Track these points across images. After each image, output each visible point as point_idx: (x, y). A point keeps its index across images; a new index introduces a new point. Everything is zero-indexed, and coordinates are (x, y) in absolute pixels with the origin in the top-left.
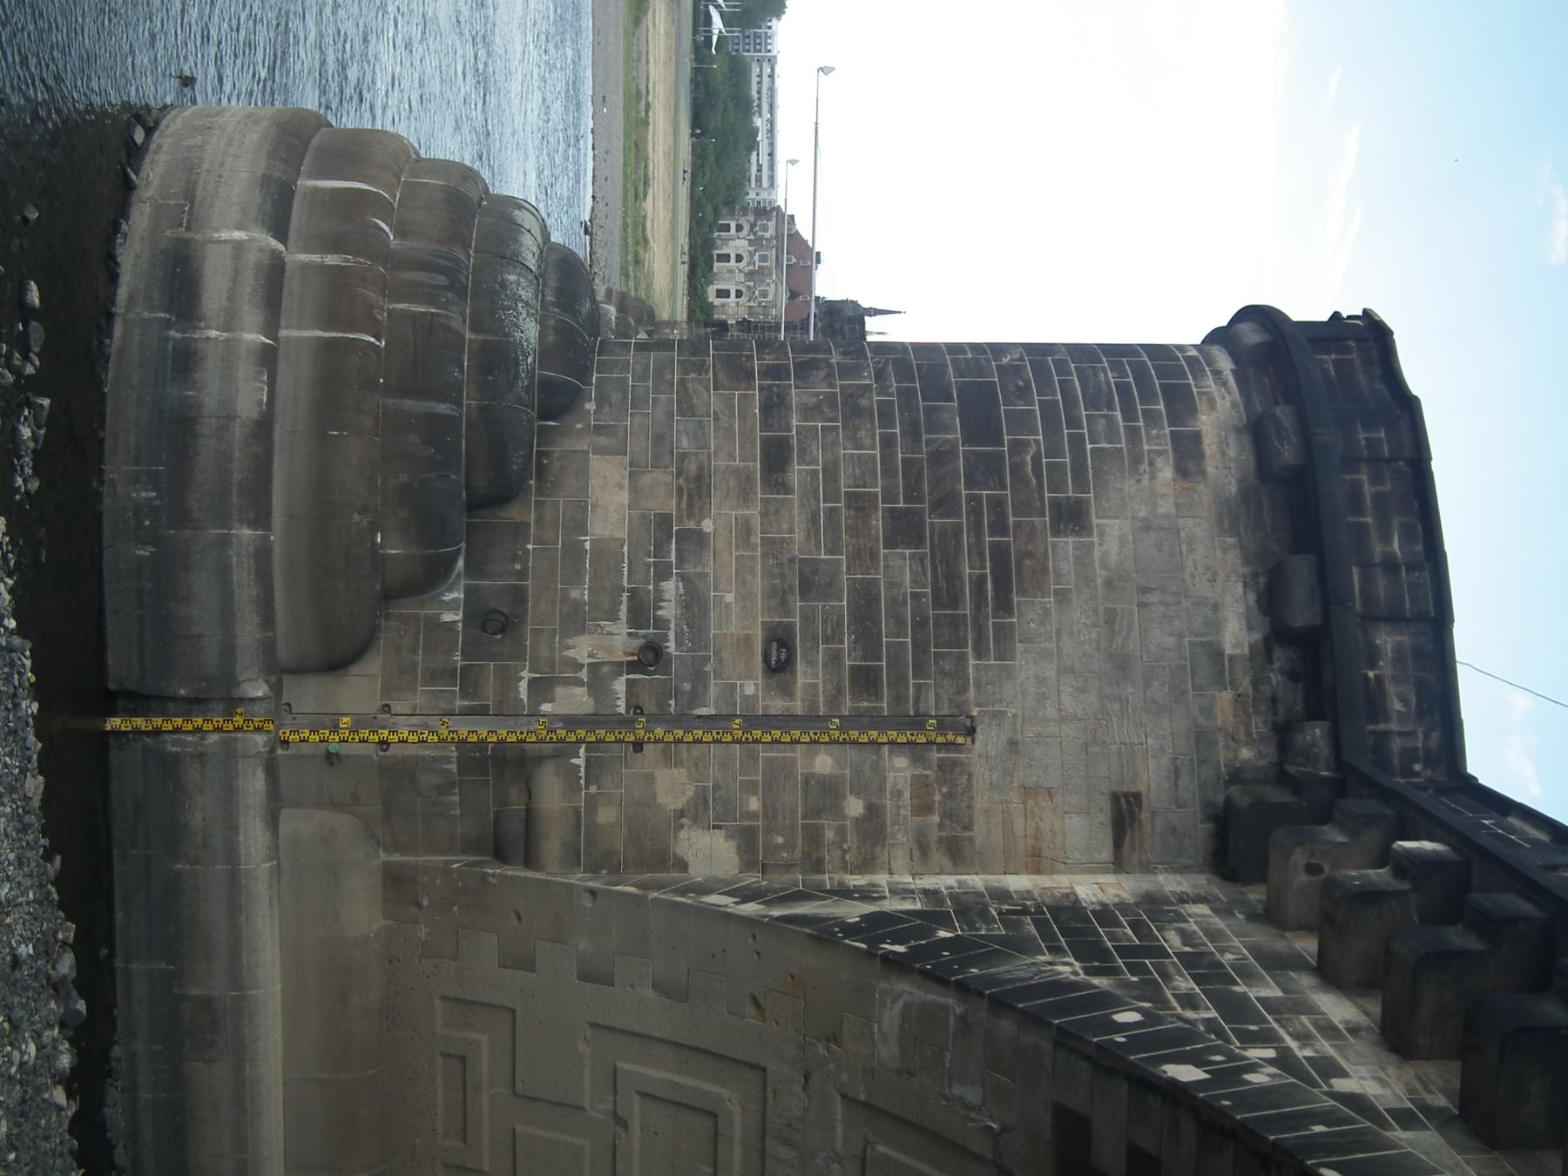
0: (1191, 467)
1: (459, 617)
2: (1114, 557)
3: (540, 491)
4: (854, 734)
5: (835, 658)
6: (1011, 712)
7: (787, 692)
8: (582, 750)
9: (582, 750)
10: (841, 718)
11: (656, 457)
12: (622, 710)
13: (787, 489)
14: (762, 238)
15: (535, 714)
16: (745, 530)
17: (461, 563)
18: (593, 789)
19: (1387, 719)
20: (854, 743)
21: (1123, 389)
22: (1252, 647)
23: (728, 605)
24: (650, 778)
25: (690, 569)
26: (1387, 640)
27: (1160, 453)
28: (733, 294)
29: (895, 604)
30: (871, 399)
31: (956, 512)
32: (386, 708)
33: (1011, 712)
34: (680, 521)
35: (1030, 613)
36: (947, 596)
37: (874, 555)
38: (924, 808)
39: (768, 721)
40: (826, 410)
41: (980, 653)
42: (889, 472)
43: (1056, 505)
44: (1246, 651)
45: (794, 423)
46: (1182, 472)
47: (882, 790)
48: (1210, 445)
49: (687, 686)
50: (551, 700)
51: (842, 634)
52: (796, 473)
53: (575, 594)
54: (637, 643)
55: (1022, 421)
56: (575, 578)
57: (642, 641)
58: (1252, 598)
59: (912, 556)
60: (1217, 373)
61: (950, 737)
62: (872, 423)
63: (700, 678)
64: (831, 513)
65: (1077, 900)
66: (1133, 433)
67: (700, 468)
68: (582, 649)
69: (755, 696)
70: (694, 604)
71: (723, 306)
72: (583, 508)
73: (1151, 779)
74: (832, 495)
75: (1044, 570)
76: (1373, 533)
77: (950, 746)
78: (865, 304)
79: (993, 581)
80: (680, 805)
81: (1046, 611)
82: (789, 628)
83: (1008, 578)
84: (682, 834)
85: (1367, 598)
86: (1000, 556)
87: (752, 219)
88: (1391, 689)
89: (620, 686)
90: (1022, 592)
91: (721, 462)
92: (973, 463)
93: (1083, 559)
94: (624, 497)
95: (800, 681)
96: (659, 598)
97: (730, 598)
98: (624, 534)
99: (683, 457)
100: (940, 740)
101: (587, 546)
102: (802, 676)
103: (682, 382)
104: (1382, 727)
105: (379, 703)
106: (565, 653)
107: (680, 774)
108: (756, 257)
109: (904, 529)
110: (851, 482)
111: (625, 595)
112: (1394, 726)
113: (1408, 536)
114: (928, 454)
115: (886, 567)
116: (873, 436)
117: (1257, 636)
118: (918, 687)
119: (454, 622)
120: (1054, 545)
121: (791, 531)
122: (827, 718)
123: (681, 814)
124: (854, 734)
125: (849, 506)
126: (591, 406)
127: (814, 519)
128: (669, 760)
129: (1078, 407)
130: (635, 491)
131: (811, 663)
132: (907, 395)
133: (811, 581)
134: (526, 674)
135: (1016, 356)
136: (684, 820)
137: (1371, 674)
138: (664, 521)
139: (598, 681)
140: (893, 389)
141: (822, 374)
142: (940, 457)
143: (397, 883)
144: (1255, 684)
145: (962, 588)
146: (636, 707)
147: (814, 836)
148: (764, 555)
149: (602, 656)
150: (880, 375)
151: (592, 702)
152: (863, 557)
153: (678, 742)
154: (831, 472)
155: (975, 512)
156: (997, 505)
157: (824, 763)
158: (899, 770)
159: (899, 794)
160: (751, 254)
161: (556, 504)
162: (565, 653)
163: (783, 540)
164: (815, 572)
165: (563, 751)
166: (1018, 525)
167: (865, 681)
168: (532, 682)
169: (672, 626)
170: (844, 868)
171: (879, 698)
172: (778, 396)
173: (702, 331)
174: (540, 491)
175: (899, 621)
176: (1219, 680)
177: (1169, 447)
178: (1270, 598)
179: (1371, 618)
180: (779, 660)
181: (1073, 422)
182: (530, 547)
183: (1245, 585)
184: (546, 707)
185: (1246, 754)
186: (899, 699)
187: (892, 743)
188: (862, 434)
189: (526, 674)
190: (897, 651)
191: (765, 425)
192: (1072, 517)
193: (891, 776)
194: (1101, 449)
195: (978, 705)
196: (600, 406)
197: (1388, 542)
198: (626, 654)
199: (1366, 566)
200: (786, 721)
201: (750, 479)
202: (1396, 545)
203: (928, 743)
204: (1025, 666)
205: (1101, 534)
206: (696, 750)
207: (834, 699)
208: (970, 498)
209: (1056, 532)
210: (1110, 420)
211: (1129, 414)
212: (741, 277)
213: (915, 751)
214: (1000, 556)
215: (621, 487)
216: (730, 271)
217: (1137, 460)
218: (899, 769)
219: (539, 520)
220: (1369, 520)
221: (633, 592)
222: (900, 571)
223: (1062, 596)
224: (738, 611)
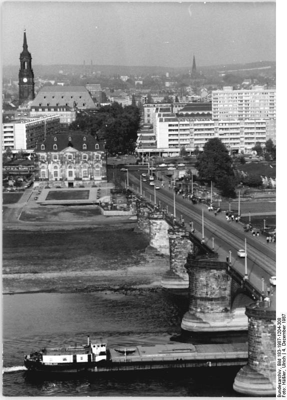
28: (70, 170)
71: (76, 174)
78: (22, 50)
87: (39, 163)
108: (55, 160)
160: (54, 162)
212: (64, 167)
216: (62, 171)
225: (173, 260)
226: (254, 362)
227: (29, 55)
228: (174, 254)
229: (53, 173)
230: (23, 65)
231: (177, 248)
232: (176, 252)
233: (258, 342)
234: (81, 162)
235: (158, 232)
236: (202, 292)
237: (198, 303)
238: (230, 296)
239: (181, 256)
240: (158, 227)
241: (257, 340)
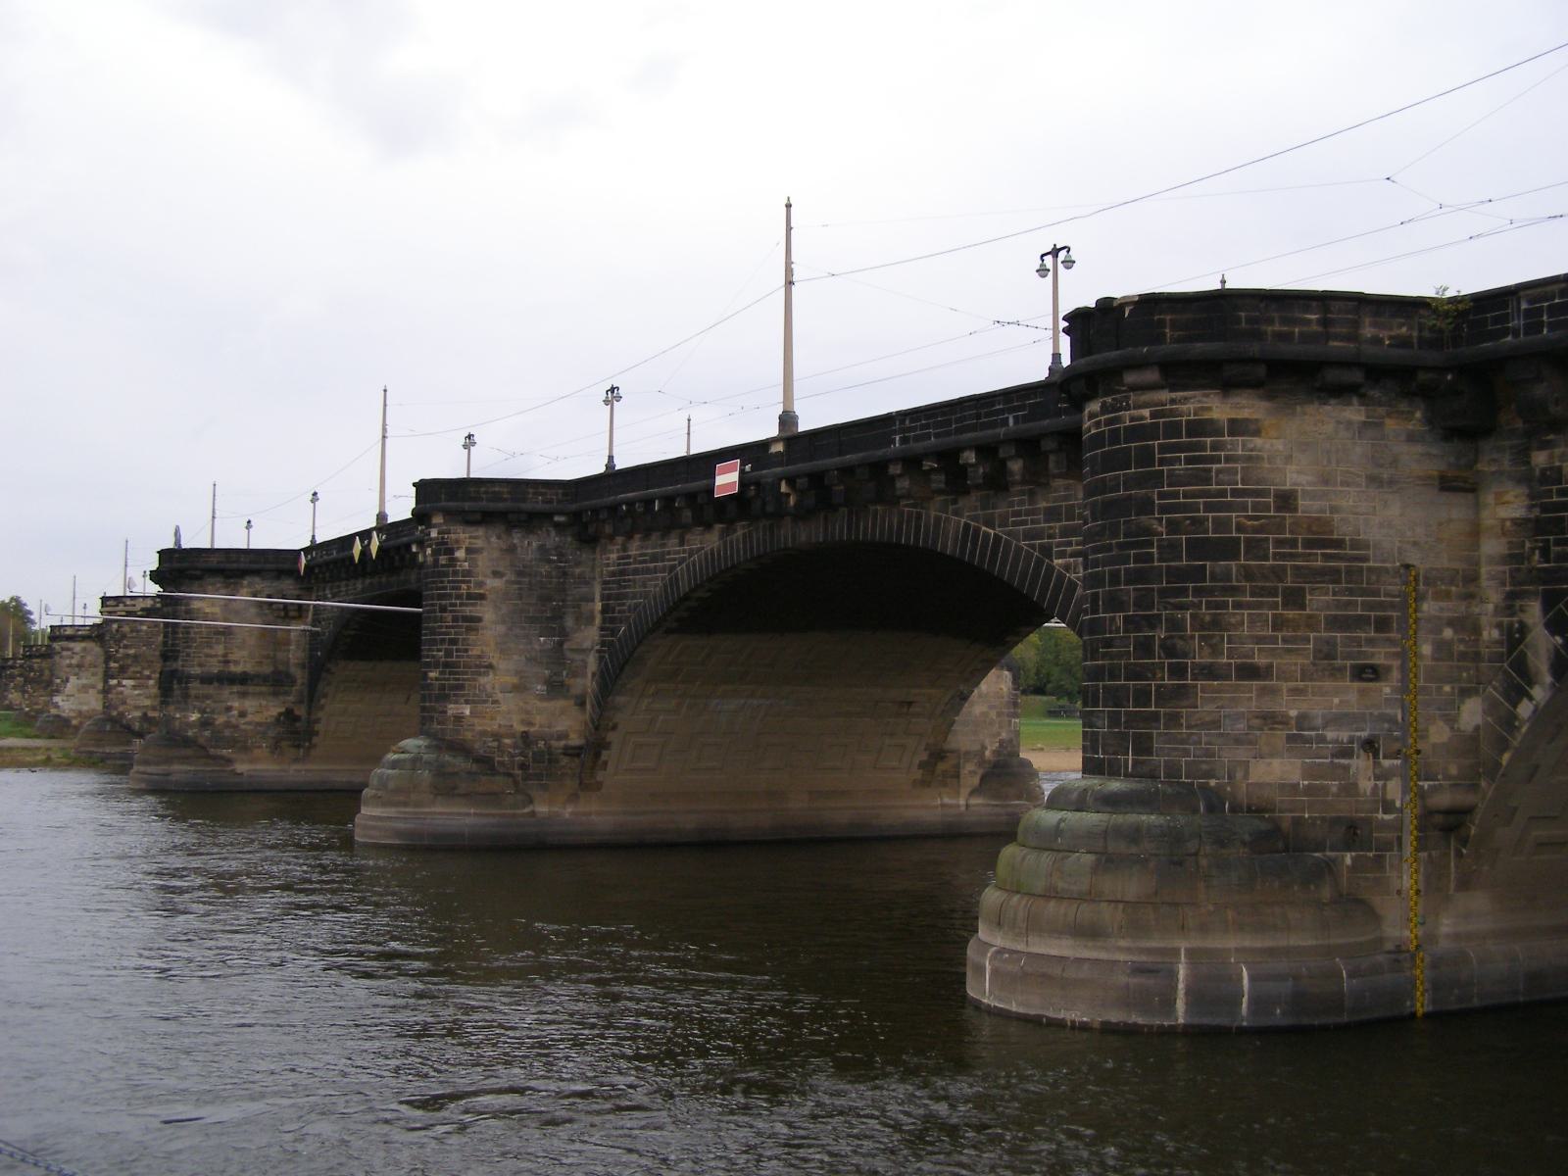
0: (1253, 427)
1: (1348, 855)
2: (1309, 478)
3: (1273, 811)
4: (1411, 632)
5: (1371, 642)
6: (1397, 544)
7: (1388, 669)
8: (1420, 783)
9: (1420, 783)
10: (1402, 639)
11: (1250, 743)
12: (1399, 761)
13: (1271, 666)
15: (1401, 810)
16: (1296, 691)
17: (1317, 854)
18: (1440, 777)
19: (1410, 336)
20: (1415, 633)
21: (1189, 461)
22: (1361, 404)
23: (1341, 701)
24: (1434, 745)
25: (1319, 722)
26: (1368, 331)
27: (1244, 445)
29: (1339, 605)
30: (1204, 614)
31: (1284, 568)
33: (1397, 544)
34: (1290, 729)
35: (1343, 530)
36: (1333, 576)
37: (1310, 617)
38: (1447, 595)
39: (1404, 679)
40: (1214, 641)
41: (1365, 559)
42: (1259, 606)
43: (1278, 509)
44: (1363, 408)
45: (1225, 660)
46: (1257, 433)
47: (1439, 618)
49: (1386, 726)
50: (1393, 802)
51: (1356, 637)
52: (1260, 660)
53: (1334, 789)
55: (1221, 525)
56: (1325, 790)
57: (1362, 751)
59: (1311, 594)
60: (1173, 401)
61: (1412, 578)
62: (1225, 614)
63: (1383, 718)
64: (1285, 641)
65: (1527, 520)
66: (1228, 459)
67: (1257, 717)
68: (1366, 785)
69: (1391, 687)
72: (1282, 787)
73: (1434, 468)
74: (1274, 640)
75: (1318, 519)
76: (1305, 329)
77: (1416, 579)
79: (1326, 548)
80: (1447, 729)
81: (1342, 519)
82: (1352, 666)
83: (1322, 538)
84: (1462, 728)
85: (1349, 338)
86: (1309, 544)
89: (1386, 763)
90: (1332, 532)
91: (1254, 706)
92: (1248, 556)
93: (1313, 496)
94: (1276, 763)
96: (1336, 741)
97: (1336, 701)
98: (1298, 762)
99: (1250, 727)
100: (1413, 584)
101: (1306, 783)
102: (1379, 657)
103: (1188, 728)
104: (1415, 341)
105: (1396, 896)
106: (1368, 793)
107: (1432, 729)
109: (1295, 599)
110: (1266, 628)
111: (1336, 761)
112: (1415, 334)
113: (1308, 310)
114: (1247, 581)
115: (1317, 610)
116: (1235, 614)
117: (1355, 400)
119: (1352, 858)
120: (1303, 512)
121: (1296, 664)
122: (1403, 648)
123: (1452, 728)
124: (1411, 632)
125: (1281, 630)
126: (1213, 782)
127: (1289, 651)
128: (1424, 737)
129: (1209, 489)
130: (1272, 755)
131: (1373, 655)
132: (1198, 592)
133: (1326, 653)
134: (1380, 815)
135: (1155, 522)
136: (1456, 726)
137: (1387, 342)
138: (1291, 738)
139: (1383, 776)
140: (1195, 600)
141: (1180, 644)
142: (1248, 574)
143: (1464, 884)
144: (1380, 406)
145: (1330, 567)
146: (1396, 754)
147: (1463, 656)
148: (1311, 680)
149: (1370, 773)
151: (1395, 779)
152: (1311, 623)
153: (1416, 730)
154: (1259, 640)
155: (1283, 557)
156: (1279, 543)
157: (1426, 649)
158: (1429, 607)
159: (1442, 609)
161: (1282, 802)
162: (1368, 793)
163: (1301, 670)
164: (1320, 651)
165: (1422, 795)
166: (1291, 532)
167: (1383, 625)
168: (1385, 813)
169: (1352, 734)
170: (1477, 640)
171: (1392, 617)
172: (1203, 669)
173: (177, 692)
174: (1273, 811)
175: (1349, 604)
176: (1380, 425)
177: (1240, 439)
179: (1353, 337)
180: (1367, 673)
181: (1222, 493)
182: (1307, 816)
183: (1325, 404)
184: (1398, 804)
185: (1418, 415)
186: (1392, 606)
187: (1416, 611)
188: (1233, 620)
189: (1380, 815)
190: (1367, 606)
191: (1228, 677)
192: (1286, 500)
193: (1433, 612)
194: (1242, 479)
195: (1395, 562)
196: (1213, 777)
198: (1369, 759)
199: (1328, 337)
200: (1403, 669)
202: (1314, 317)
203: (1415, 590)
204: (1372, 534)
205: (1298, 485)
206: (1420, 719)
207: (1392, 642)
208: (1275, 559)
209: (1295, 510)
210: (1219, 472)
211: (1217, 460)
213: (1420, 598)
214: (1309, 544)
215: (1270, 764)
217: (1249, 459)
218: (1429, 607)
219: (1291, 811)
220: (1297, 330)
221: (1334, 756)
222: (1320, 601)
223: (1334, 509)
224: (1345, 696)
225: (114, 682)
226: (452, 709)
228: (116, 665)
231: (126, 647)
232: (122, 658)
233: (466, 619)
235: (76, 674)
236: (207, 656)
237: (193, 692)
238: (303, 666)
239: (139, 669)
240: (74, 662)
241: (468, 611)
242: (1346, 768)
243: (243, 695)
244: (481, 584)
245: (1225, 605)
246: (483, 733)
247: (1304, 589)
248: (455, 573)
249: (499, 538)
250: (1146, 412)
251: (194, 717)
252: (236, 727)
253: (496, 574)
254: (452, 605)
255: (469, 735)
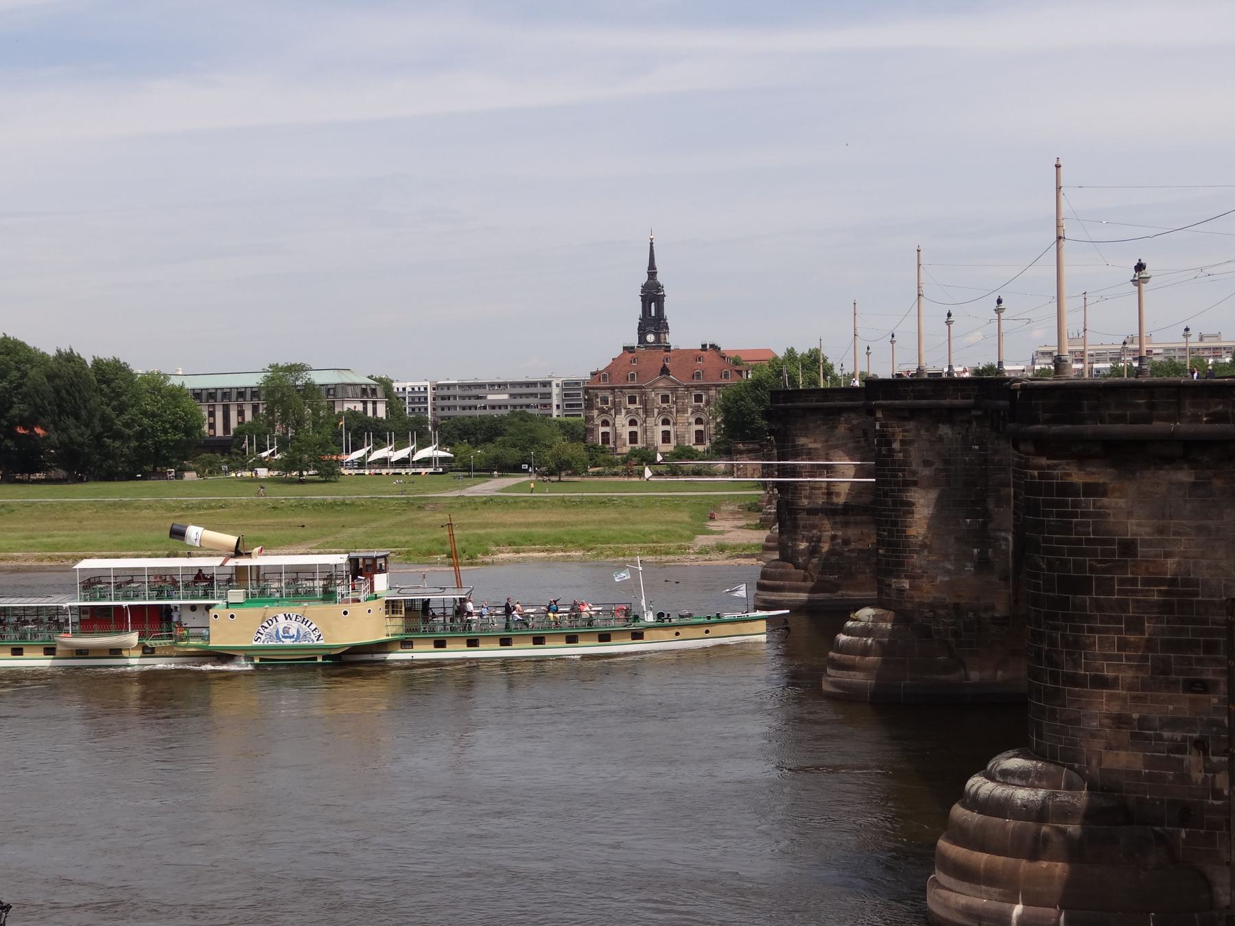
2: (1148, 530)
5: (1200, 661)
7: (1216, 683)
13: (1117, 678)
14: (614, 403)
15: (1229, 797)
17: (1157, 828)
21: (1059, 515)
25: (1157, 723)
28: (667, 428)
31: (1126, 602)
32: (1228, 864)
33: (1224, 582)
41: (1196, 594)
42: (1107, 631)
46: (1104, 494)
48: (1089, 480)
53: (1171, 778)
54: (1194, 751)
58: (1167, 467)
60: (1049, 467)
66: (1084, 515)
68: (1198, 776)
70: (1174, 724)
71: (677, 437)
74: (1119, 658)
78: (644, 278)
87: (596, 413)
88: (1211, 411)
89: (1215, 759)
90: (1166, 573)
93: (1149, 544)
94: (1123, 754)
95: (1211, 677)
96: (1171, 740)
97: (1171, 707)
99: (1101, 725)
103: (1061, 722)
108: (632, 407)
118: (1214, 623)
130: (1118, 748)
134: (1210, 801)
138: (1134, 736)
142: (1099, 606)
149: (1201, 766)
150: (1056, 628)
154: (1108, 658)
156: (1123, 582)
167: (1210, 648)
178: (1168, 461)
181: (1079, 542)
184: (1226, 792)
192: (1128, 547)
197: (1139, 405)
201: (1112, 695)
209: (1136, 555)
210: (1077, 524)
211: (1075, 515)
214: (1146, 582)
216: (645, 431)
217: (1098, 515)
221: (1169, 751)
224: (1179, 704)
227: (658, 287)
229: (626, 437)
230: (646, 309)
234: (690, 410)
237: (801, 523)
242: (1181, 761)
243: (846, 524)
244: (914, 473)
245: (1081, 630)
246: (921, 604)
247: (1142, 618)
248: (894, 462)
249: (927, 430)
250: (1036, 473)
251: (803, 545)
252: (840, 554)
253: (927, 463)
254: (892, 491)
255: (909, 606)
